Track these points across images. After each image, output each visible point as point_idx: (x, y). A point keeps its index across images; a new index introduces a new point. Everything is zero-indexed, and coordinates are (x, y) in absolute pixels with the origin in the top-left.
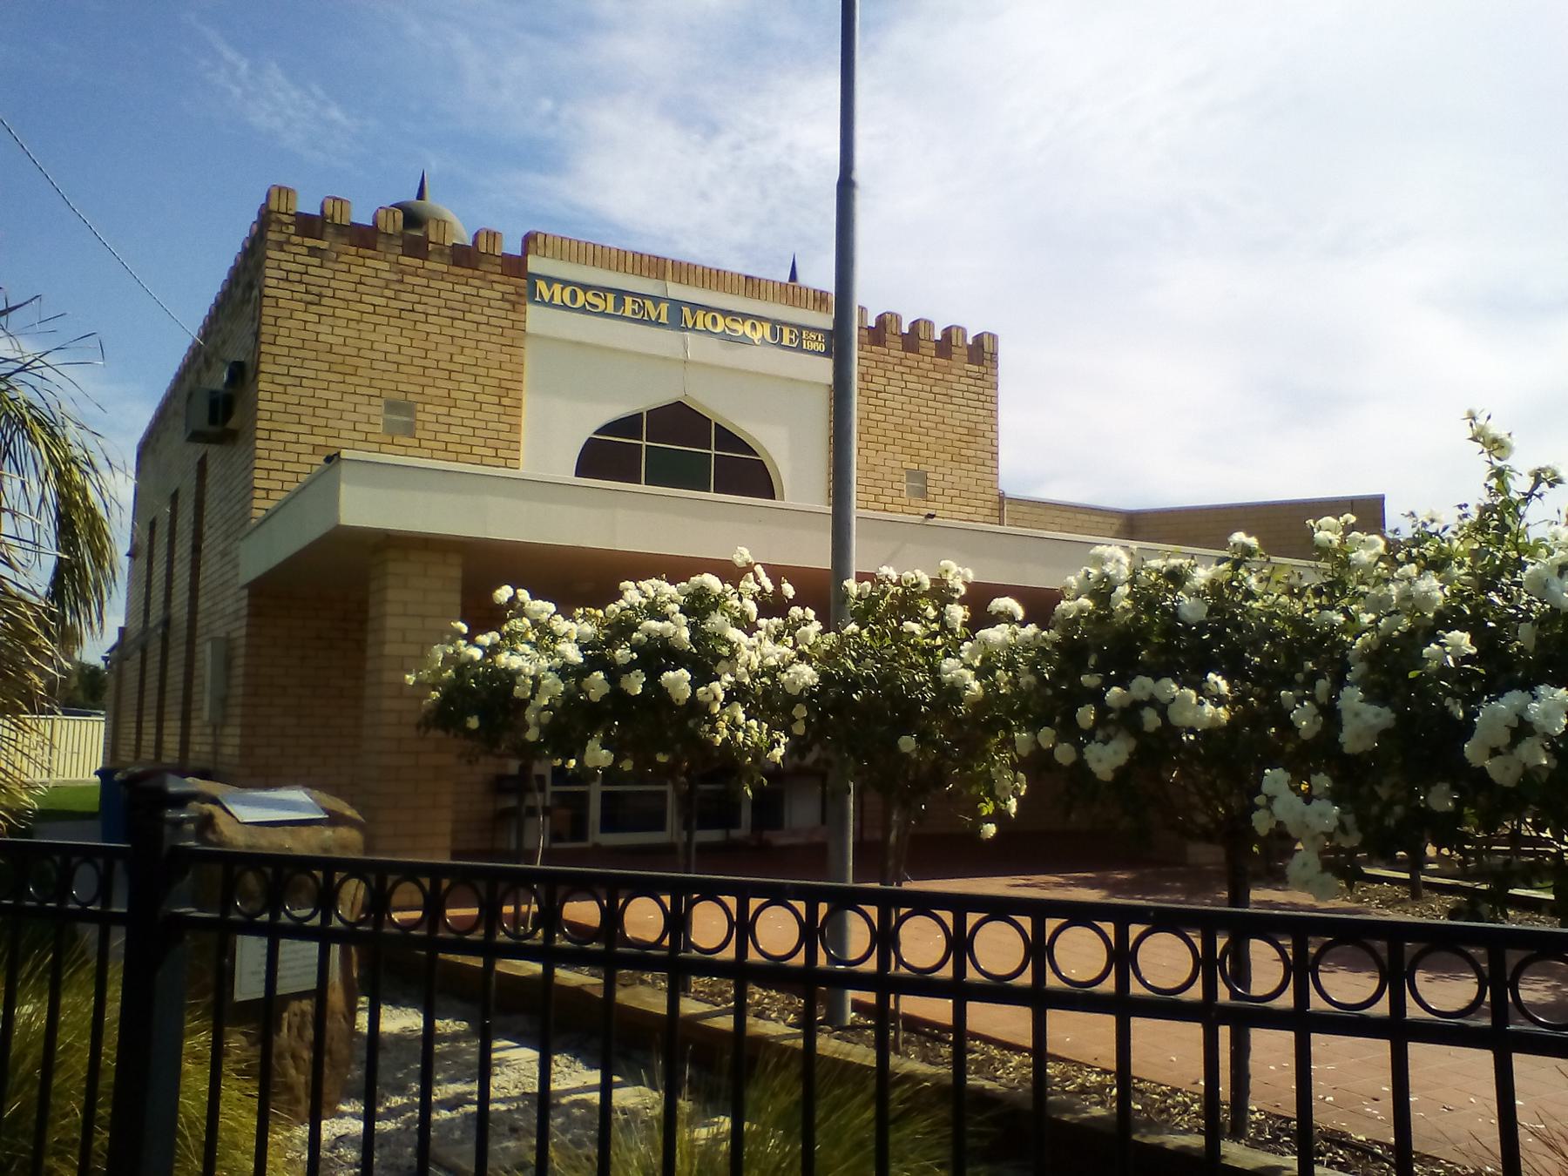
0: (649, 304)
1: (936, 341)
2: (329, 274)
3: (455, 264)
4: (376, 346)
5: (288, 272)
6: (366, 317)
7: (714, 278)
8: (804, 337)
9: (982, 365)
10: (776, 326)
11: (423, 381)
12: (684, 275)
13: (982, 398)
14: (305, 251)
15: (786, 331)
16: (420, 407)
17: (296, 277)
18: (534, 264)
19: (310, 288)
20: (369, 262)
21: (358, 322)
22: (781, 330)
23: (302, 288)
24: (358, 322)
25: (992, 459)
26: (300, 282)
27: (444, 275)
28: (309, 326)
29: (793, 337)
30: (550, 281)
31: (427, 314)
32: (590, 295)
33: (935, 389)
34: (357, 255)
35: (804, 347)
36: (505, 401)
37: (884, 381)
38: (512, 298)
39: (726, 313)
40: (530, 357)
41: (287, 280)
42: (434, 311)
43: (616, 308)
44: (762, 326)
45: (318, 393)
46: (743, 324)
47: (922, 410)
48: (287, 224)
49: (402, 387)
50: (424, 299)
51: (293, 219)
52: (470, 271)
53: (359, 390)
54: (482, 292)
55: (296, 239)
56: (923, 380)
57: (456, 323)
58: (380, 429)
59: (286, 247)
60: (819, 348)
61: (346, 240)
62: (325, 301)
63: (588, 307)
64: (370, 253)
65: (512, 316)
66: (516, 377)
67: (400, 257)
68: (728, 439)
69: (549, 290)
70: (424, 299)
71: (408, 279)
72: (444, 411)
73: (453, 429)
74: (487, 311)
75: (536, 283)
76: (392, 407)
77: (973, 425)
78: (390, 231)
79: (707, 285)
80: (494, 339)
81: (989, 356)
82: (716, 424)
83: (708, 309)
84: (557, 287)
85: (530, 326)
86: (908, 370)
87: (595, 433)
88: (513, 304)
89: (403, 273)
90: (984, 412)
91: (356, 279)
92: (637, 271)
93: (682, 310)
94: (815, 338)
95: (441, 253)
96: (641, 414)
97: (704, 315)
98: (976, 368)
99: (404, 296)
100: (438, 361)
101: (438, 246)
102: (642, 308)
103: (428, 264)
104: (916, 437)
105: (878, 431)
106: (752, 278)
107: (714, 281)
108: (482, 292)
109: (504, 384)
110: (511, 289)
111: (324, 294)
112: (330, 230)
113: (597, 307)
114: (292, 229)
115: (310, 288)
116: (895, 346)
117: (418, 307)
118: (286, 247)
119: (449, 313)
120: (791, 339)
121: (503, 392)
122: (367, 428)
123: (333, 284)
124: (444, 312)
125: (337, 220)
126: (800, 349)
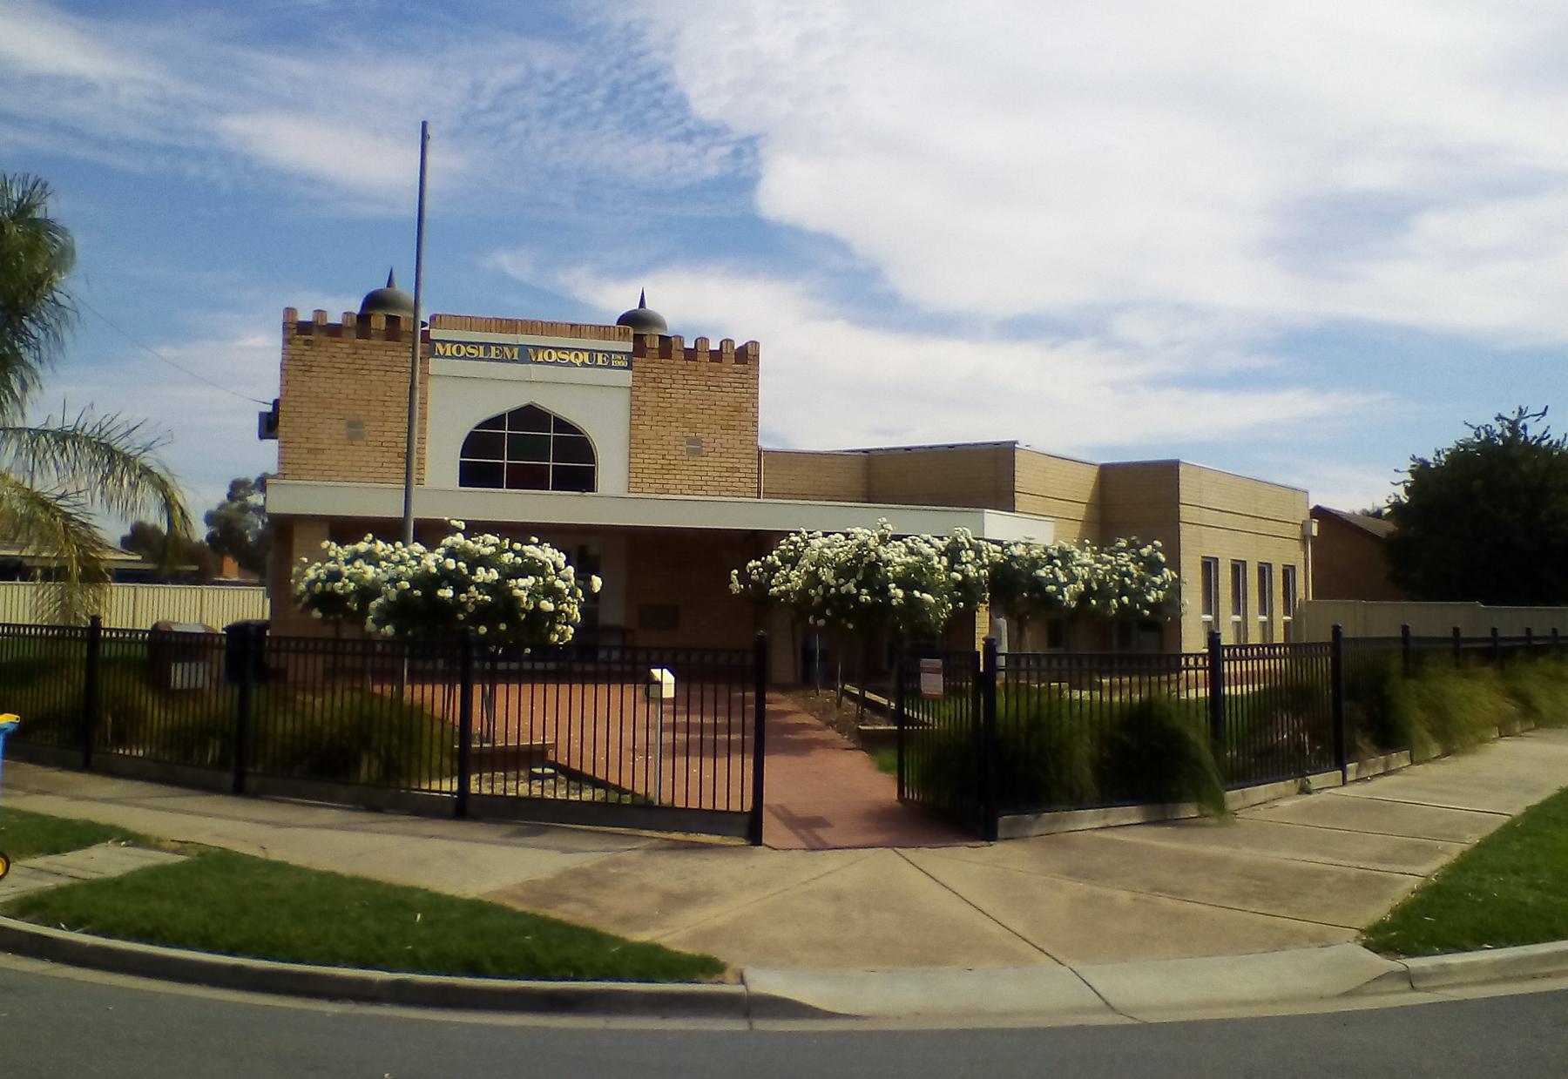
1: (710, 351)
7: (551, 328)
13: (745, 386)
14: (302, 342)
15: (600, 356)
18: (435, 334)
20: (338, 345)
21: (332, 378)
22: (597, 355)
23: (301, 363)
25: (753, 426)
26: (300, 360)
29: (605, 359)
30: (443, 342)
33: (709, 383)
40: (433, 387)
59: (293, 341)
60: (623, 365)
62: (314, 369)
63: (468, 355)
64: (337, 339)
68: (562, 425)
72: (380, 424)
76: (351, 425)
77: (738, 404)
81: (751, 358)
84: (448, 345)
87: (476, 428)
96: (504, 415)
103: (371, 342)
112: (315, 329)
114: (295, 331)
116: (679, 358)
117: (366, 367)
118: (293, 341)
119: (383, 368)
120: (603, 361)
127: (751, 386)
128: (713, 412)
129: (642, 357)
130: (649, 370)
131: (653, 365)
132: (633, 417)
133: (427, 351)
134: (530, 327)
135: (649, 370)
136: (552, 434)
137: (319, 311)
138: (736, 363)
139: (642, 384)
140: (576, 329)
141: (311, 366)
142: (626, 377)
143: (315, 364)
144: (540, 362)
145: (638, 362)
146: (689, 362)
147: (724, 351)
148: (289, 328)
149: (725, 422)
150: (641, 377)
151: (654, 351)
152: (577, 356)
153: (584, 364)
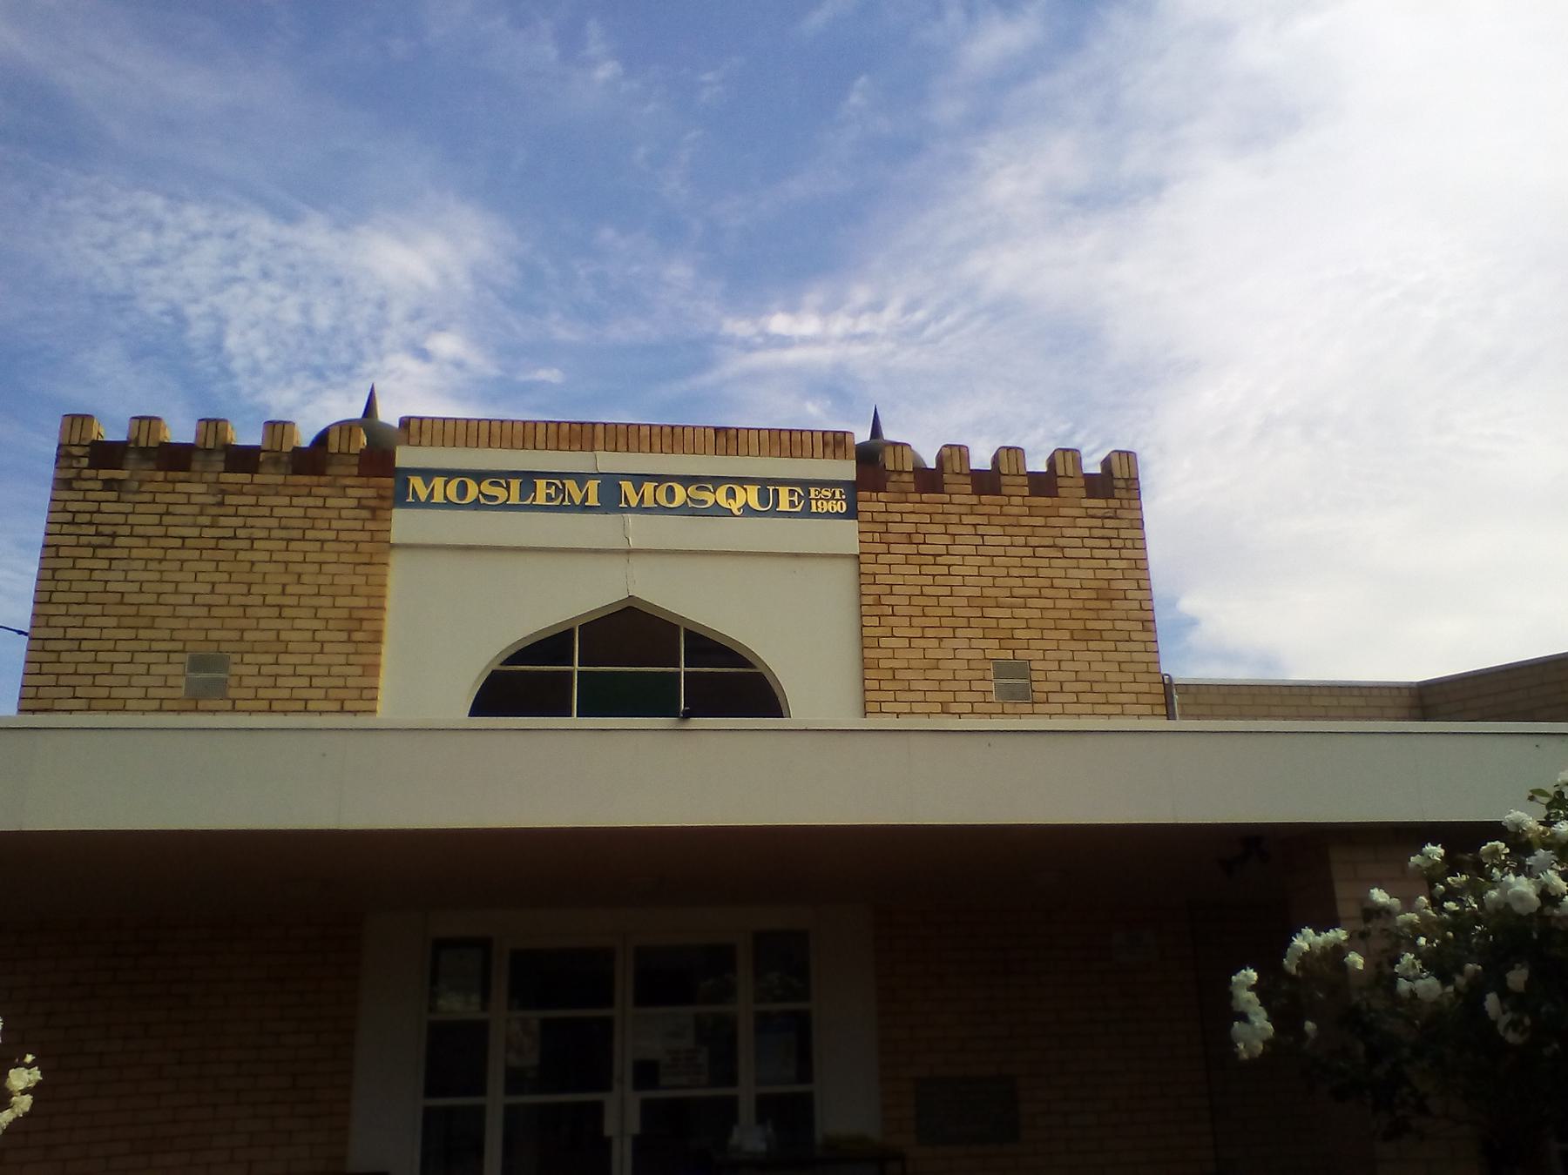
0: (571, 485)
2: (127, 508)
3: (296, 472)
4: (182, 588)
5: (74, 513)
6: (170, 554)
7: (671, 438)
8: (812, 496)
9: (1113, 497)
10: (766, 485)
11: (243, 623)
12: (622, 441)
13: (1116, 543)
14: (99, 485)
15: (784, 492)
16: (236, 658)
17: (86, 517)
18: (405, 457)
19: (101, 528)
20: (180, 487)
21: (160, 561)
22: (776, 492)
23: (92, 530)
24: (160, 561)
25: (1145, 630)
26: (90, 523)
27: (280, 488)
28: (96, 575)
29: (795, 498)
30: (428, 474)
31: (252, 540)
32: (486, 487)
33: (1033, 541)
34: (166, 481)
35: (814, 509)
36: (358, 636)
37: (947, 539)
38: (373, 503)
39: (686, 481)
40: (399, 575)
41: (73, 523)
42: (264, 534)
43: (523, 496)
44: (745, 489)
45: (102, 657)
46: (715, 493)
47: (1014, 572)
48: (78, 457)
49: (214, 635)
50: (250, 522)
51: (88, 449)
52: (315, 479)
53: (155, 646)
54: (331, 502)
55: (91, 473)
56: (1009, 530)
57: (293, 545)
58: (181, 693)
59: (75, 484)
60: (837, 508)
61: (152, 465)
62: (119, 542)
63: (483, 500)
64: (182, 475)
65: (370, 525)
66: (373, 602)
67: (221, 475)
68: (706, 647)
69: (427, 487)
70: (250, 522)
71: (229, 499)
72: (270, 658)
73: (281, 681)
74: (335, 524)
75: (409, 480)
76: (199, 663)
77: (1104, 584)
78: (210, 445)
79: (657, 447)
80: (344, 558)
82: (685, 628)
83: (659, 479)
84: (438, 482)
85: (394, 538)
86: (984, 520)
87: (506, 663)
88: (373, 510)
89: (224, 493)
90: (1123, 564)
91: (162, 509)
92: (552, 444)
93: (620, 486)
94: (830, 495)
95: (276, 462)
96: (570, 632)
97: (656, 487)
98: (1101, 503)
99: (223, 521)
100: (264, 596)
101: (273, 454)
102: (561, 490)
103: (258, 478)
104: (1007, 613)
105: (939, 612)
106: (726, 429)
107: (667, 441)
108: (331, 502)
109: (362, 614)
110: (371, 492)
111: (118, 533)
112: (132, 456)
113: (496, 498)
114: (85, 462)
115: (101, 528)
119: (283, 534)
120: (792, 502)
121: (354, 625)
122: (162, 693)
123: (132, 519)
124: (276, 533)
125: (143, 443)
126: (807, 513)
127: (1129, 544)
128: (1049, 603)
129: (878, 492)
130: (897, 518)
131: (908, 507)
132: (867, 621)
133: (389, 493)
134: (623, 437)
135: (897, 518)
136: (683, 669)
137: (141, 419)
138: (1091, 495)
139: (883, 548)
140: (727, 439)
141: (114, 536)
142: (846, 535)
143: (126, 530)
144: (648, 510)
145: (871, 503)
146: (984, 498)
147: (1060, 472)
148: (70, 456)
149: (1079, 625)
150: (879, 534)
151: (907, 478)
152: (731, 494)
153: (747, 510)
